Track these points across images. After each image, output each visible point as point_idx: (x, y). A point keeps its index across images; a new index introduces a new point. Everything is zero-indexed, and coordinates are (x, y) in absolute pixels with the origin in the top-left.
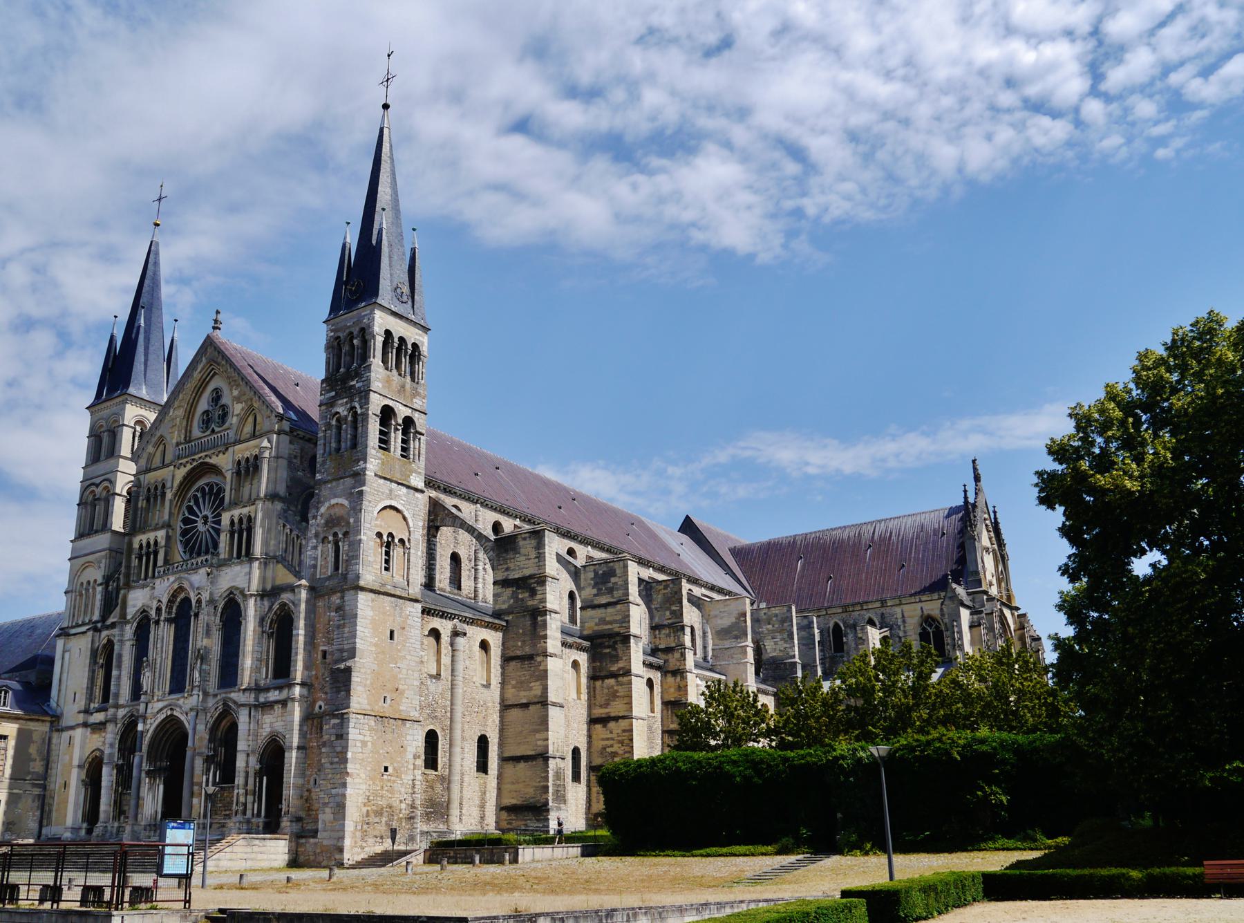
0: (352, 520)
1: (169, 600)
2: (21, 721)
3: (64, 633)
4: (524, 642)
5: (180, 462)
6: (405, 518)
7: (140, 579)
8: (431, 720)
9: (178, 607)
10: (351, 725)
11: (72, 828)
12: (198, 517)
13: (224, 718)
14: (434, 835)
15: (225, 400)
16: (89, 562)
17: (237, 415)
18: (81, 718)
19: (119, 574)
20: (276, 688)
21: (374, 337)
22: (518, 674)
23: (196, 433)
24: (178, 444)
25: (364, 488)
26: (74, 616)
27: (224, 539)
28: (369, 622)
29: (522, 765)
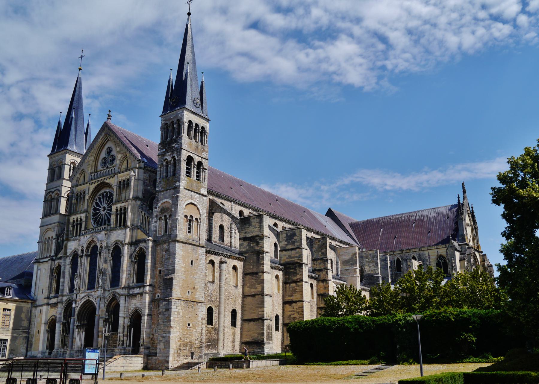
0: (173, 209)
1: (87, 246)
2: (17, 302)
3: (38, 261)
4: (253, 266)
5: (92, 181)
6: (198, 209)
7: (74, 236)
8: (210, 302)
9: (91, 249)
10: (173, 304)
11: (42, 352)
12: (101, 207)
13: (113, 301)
14: (211, 355)
15: (114, 153)
16: (49, 228)
17: (119, 160)
18: (46, 301)
19: (64, 234)
20: (137, 287)
21: (183, 124)
22: (250, 281)
23: (100, 168)
24: (91, 173)
25: (179, 194)
26: (42, 253)
27: (113, 218)
28: (181, 257)
29: (252, 323)
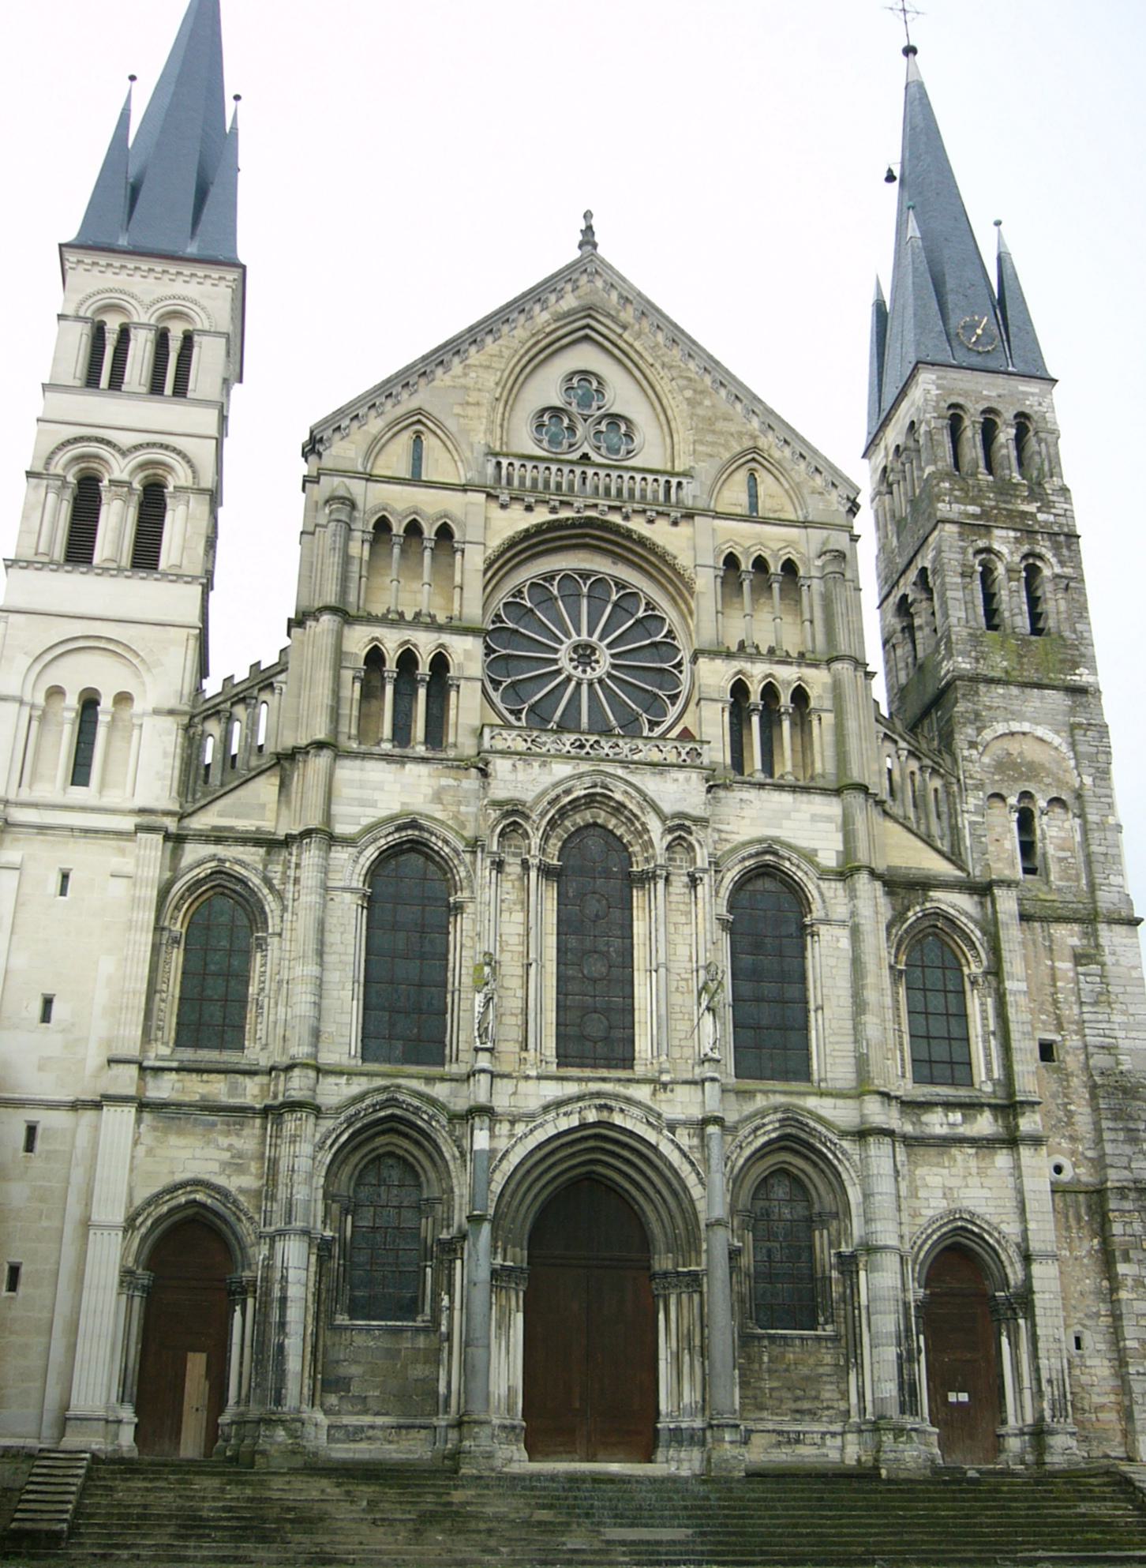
23: (525, 441)
